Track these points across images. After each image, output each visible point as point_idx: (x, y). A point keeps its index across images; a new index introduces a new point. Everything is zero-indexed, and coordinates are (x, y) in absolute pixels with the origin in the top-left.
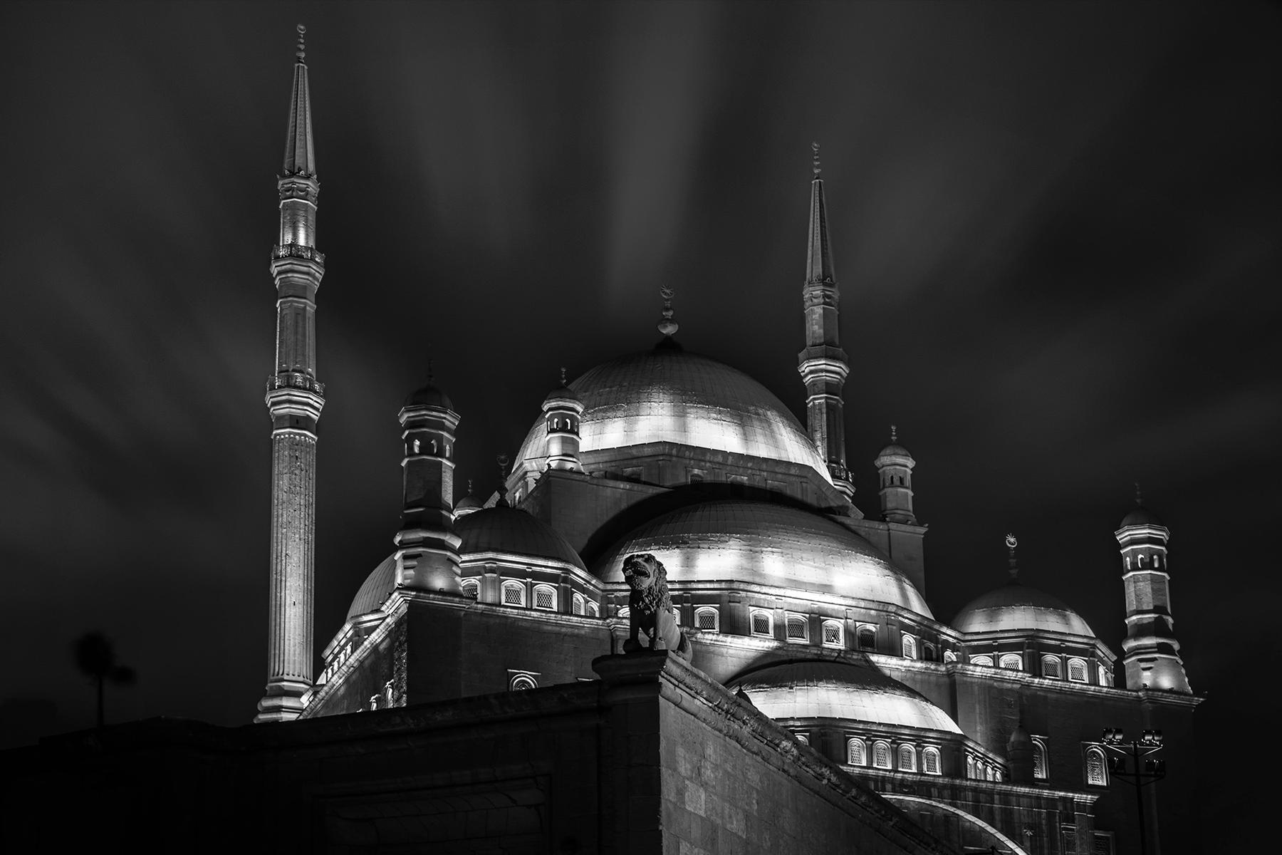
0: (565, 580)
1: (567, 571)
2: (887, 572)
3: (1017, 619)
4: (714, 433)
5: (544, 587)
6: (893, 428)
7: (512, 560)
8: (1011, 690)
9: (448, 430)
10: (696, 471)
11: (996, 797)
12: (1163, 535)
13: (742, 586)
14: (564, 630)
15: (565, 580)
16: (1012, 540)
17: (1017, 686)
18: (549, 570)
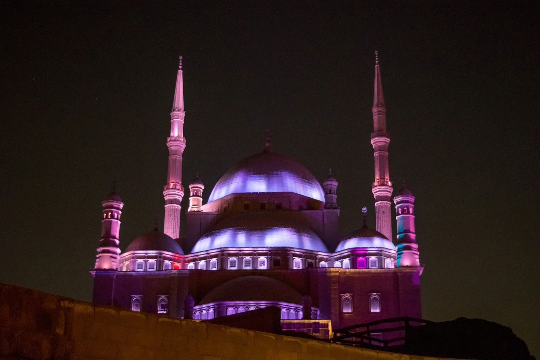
0: (160, 257)
1: (161, 253)
2: (294, 233)
3: (352, 244)
4: (258, 186)
5: (151, 261)
6: (330, 170)
7: (141, 253)
8: (335, 276)
9: (200, 196)
10: (246, 202)
11: (285, 326)
12: (412, 199)
13: (225, 249)
14: (153, 277)
15: (160, 257)
16: (364, 209)
17: (338, 274)
18: (154, 254)
